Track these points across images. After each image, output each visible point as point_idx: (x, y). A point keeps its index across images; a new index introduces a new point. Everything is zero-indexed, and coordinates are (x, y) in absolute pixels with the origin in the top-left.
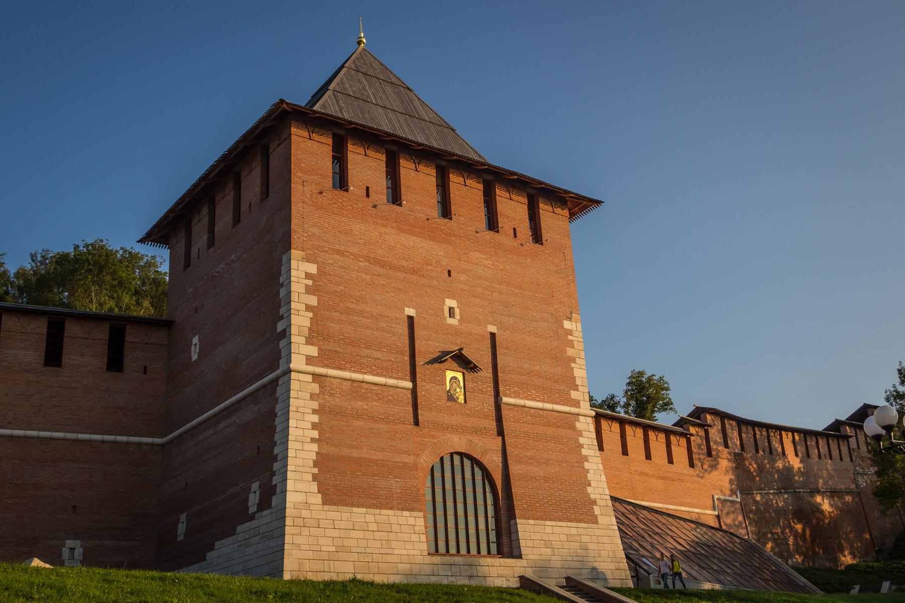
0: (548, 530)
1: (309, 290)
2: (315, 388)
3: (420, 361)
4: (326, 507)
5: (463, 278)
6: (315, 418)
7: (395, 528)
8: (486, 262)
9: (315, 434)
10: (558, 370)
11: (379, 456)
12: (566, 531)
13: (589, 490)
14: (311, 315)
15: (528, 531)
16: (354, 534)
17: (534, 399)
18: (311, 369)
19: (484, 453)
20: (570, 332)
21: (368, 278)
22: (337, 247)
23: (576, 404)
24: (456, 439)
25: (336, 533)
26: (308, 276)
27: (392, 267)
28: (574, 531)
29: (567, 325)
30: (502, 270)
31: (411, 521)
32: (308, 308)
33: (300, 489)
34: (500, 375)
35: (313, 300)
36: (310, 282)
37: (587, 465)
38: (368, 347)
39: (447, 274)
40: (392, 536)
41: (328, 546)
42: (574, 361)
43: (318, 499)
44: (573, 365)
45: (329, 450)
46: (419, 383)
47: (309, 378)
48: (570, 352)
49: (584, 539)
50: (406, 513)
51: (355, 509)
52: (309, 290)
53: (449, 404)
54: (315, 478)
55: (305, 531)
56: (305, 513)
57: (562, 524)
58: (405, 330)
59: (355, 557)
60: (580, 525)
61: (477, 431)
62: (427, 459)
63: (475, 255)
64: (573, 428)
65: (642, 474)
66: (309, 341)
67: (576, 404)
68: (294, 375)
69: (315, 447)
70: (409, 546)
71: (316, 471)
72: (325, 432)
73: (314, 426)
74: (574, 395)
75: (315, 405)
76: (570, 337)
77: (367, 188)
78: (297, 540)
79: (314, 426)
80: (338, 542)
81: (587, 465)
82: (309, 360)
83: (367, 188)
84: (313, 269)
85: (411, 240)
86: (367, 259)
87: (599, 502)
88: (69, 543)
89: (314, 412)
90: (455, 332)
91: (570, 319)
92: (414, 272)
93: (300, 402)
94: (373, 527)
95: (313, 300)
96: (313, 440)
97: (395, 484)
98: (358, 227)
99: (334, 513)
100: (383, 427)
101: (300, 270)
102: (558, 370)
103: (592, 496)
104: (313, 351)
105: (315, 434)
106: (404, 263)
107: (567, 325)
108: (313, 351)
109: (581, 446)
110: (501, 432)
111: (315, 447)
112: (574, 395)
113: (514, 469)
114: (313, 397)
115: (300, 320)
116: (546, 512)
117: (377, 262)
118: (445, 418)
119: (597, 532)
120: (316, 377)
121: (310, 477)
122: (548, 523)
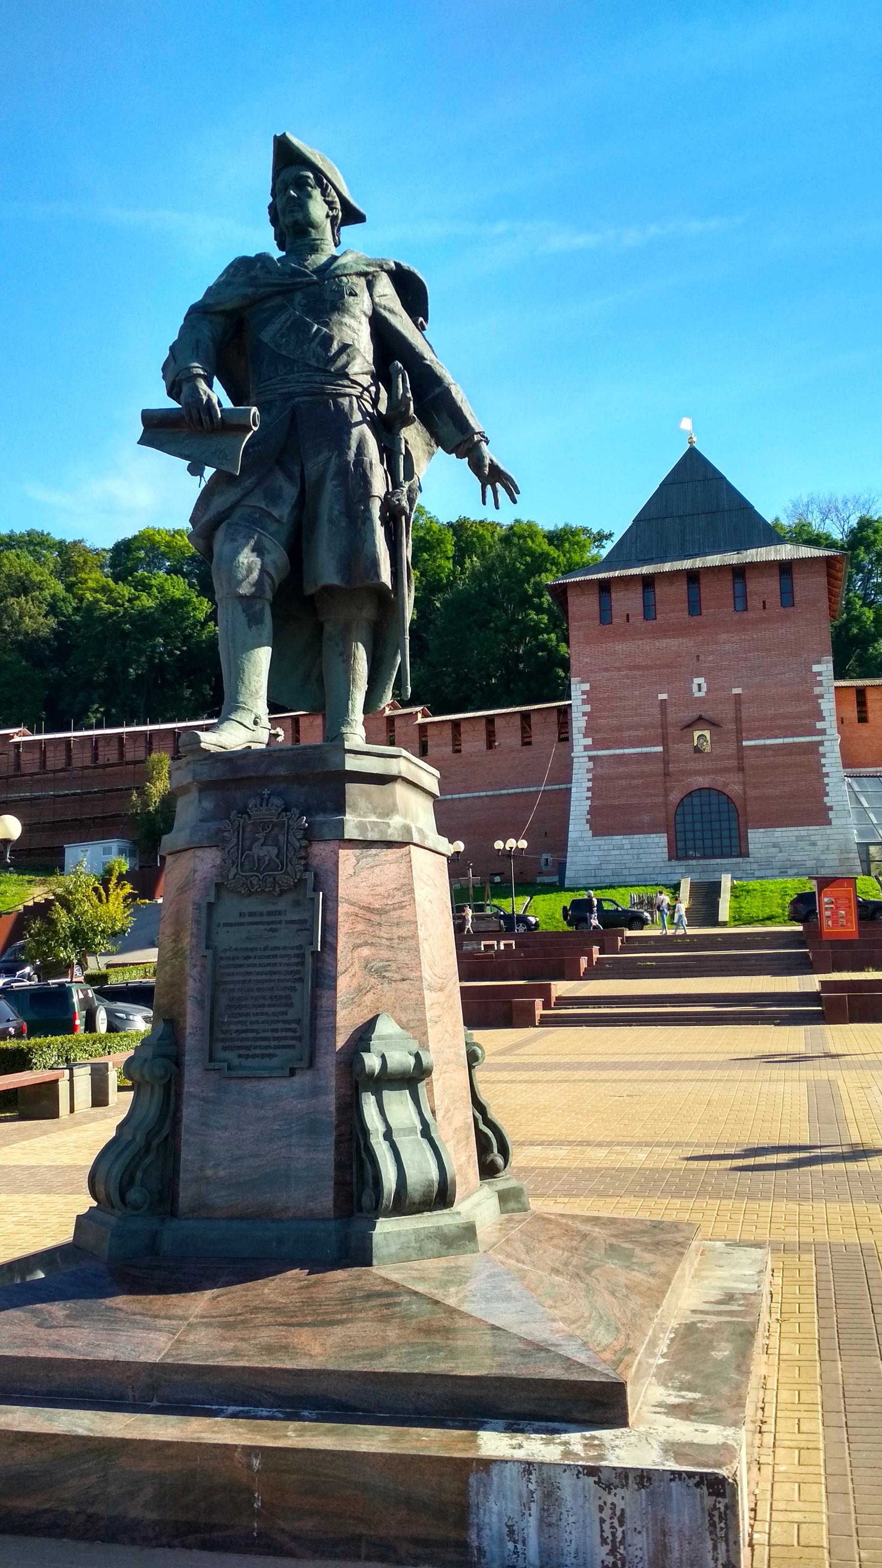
0: (777, 834)
1: (584, 702)
2: (591, 765)
3: (672, 730)
4: (595, 838)
6: (590, 784)
7: (644, 846)
8: (733, 639)
9: (590, 794)
10: (805, 708)
11: (635, 801)
12: (796, 833)
13: (826, 799)
14: (586, 718)
16: (613, 853)
17: (776, 737)
18: (586, 753)
19: (726, 785)
20: (820, 674)
22: (605, 666)
23: (823, 732)
24: (700, 779)
25: (601, 853)
26: (583, 693)
29: (816, 668)
30: (749, 641)
31: (657, 840)
32: (584, 714)
33: (578, 827)
34: (744, 725)
35: (587, 708)
36: (585, 697)
37: (826, 780)
38: (629, 728)
39: (695, 658)
40: (641, 851)
41: (594, 861)
42: (821, 696)
43: (590, 833)
44: (820, 701)
45: (597, 803)
46: (670, 745)
47: (587, 759)
48: (817, 690)
49: (813, 838)
50: (652, 835)
51: (615, 837)
52: (584, 702)
53: (697, 755)
54: (588, 821)
55: (580, 854)
56: (580, 843)
57: (792, 829)
59: (613, 866)
60: (810, 828)
62: (675, 797)
63: (724, 637)
64: (817, 752)
66: (585, 736)
68: (575, 760)
69: (589, 802)
70: (653, 856)
71: (589, 817)
73: (589, 789)
74: (819, 725)
75: (590, 776)
76: (819, 678)
77: (628, 615)
78: (574, 859)
79: (589, 789)
80: (603, 858)
81: (826, 780)
82: (586, 748)
83: (628, 615)
84: (586, 687)
85: (664, 643)
87: (834, 808)
89: (589, 780)
91: (819, 662)
92: (667, 666)
93: (580, 776)
94: (628, 846)
95: (587, 708)
96: (587, 798)
98: (620, 647)
99: (601, 841)
100: (635, 782)
101: (578, 689)
103: (828, 804)
104: (589, 741)
105: (590, 794)
106: (658, 662)
107: (816, 668)
108: (589, 741)
109: (824, 765)
111: (589, 802)
112: (819, 725)
113: (751, 793)
114: (588, 771)
115: (578, 722)
116: (774, 819)
118: (693, 766)
119: (829, 832)
120: (591, 758)
121: (585, 821)
122: (777, 829)
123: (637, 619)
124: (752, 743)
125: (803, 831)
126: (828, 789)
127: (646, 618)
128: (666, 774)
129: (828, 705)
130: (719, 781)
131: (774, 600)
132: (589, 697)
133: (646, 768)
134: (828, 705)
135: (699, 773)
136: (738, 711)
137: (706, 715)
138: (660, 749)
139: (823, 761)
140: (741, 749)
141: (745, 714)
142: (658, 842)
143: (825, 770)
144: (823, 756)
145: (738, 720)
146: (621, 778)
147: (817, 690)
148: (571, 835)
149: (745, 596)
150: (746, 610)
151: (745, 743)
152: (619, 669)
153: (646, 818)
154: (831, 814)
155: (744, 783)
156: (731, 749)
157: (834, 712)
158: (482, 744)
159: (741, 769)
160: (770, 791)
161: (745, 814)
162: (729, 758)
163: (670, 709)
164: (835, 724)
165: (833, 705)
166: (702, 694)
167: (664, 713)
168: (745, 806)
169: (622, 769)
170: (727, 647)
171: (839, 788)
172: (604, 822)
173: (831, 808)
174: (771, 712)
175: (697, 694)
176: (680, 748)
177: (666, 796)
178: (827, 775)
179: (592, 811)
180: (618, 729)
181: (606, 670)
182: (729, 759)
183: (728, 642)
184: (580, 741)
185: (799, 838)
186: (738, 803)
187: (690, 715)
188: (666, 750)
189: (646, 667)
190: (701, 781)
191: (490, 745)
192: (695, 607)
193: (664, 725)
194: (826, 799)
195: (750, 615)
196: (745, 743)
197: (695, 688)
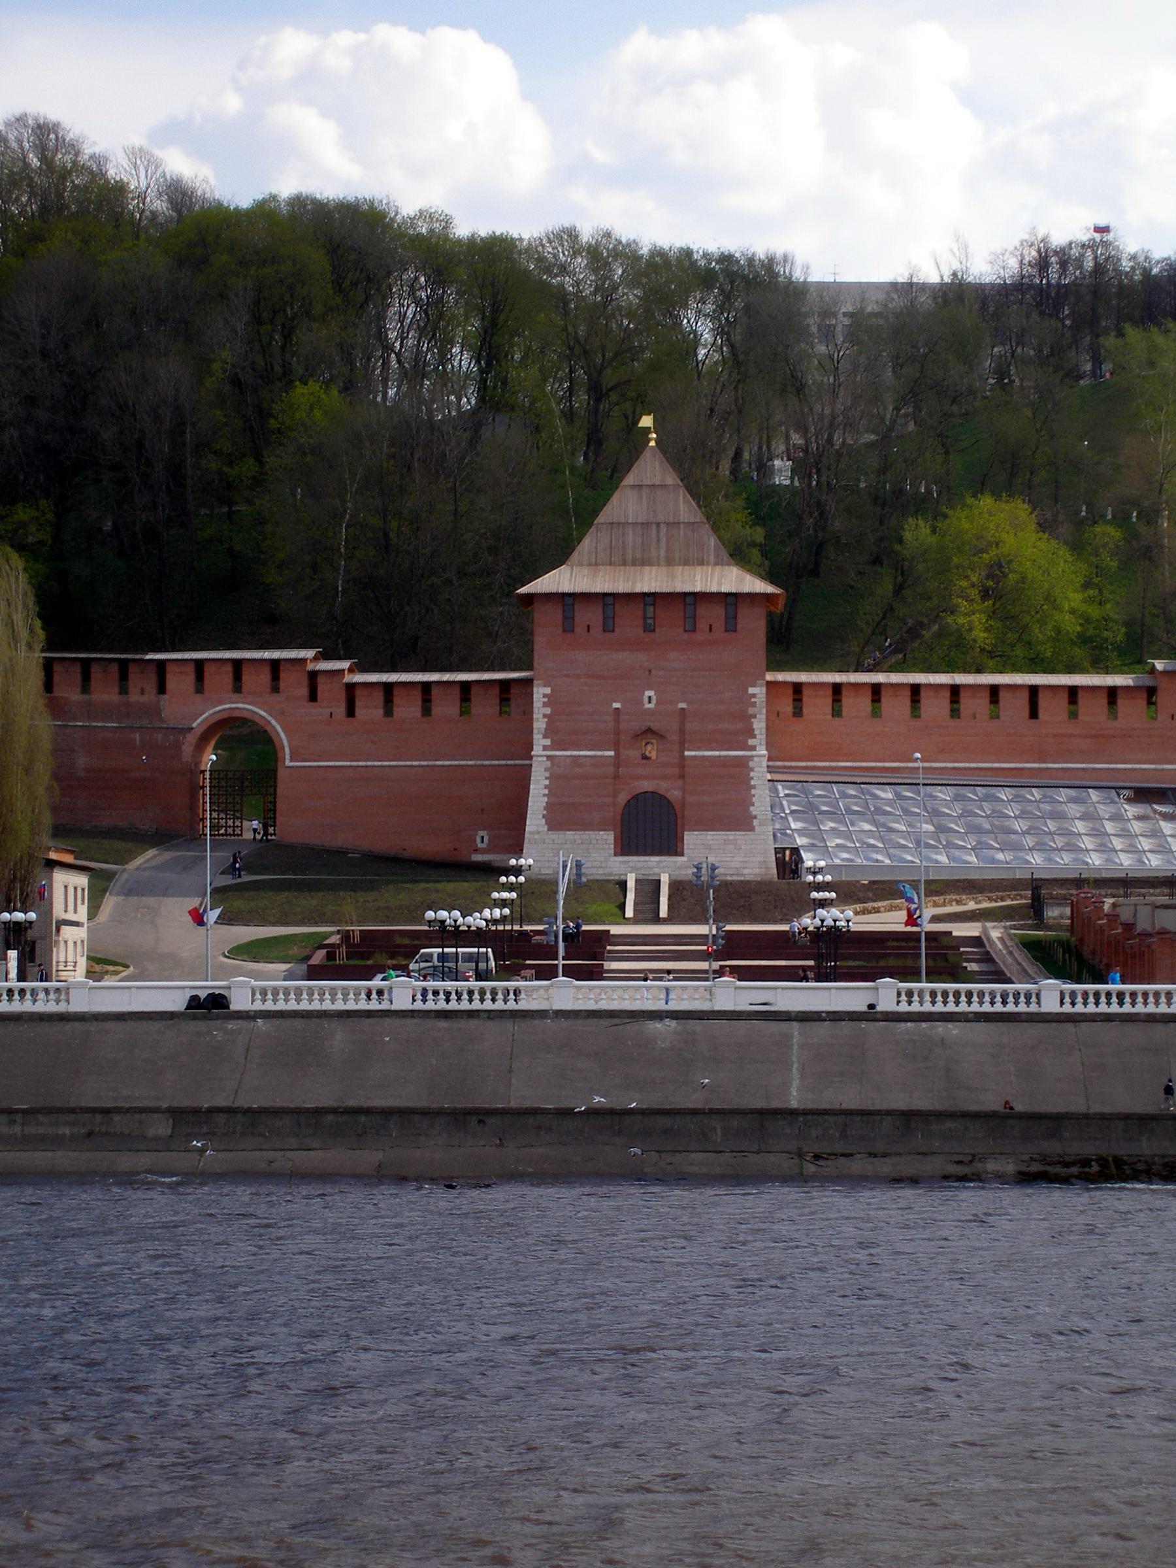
1: (545, 705)
3: (623, 737)
5: (661, 673)
6: (547, 782)
7: (594, 842)
10: (740, 725)
13: (752, 808)
15: (691, 839)
18: (545, 753)
20: (754, 696)
21: (585, 688)
26: (545, 696)
28: (731, 837)
29: (751, 690)
31: (605, 837)
32: (545, 716)
33: (535, 821)
35: (548, 711)
37: (753, 792)
42: (755, 716)
43: (546, 828)
46: (622, 750)
48: (751, 711)
52: (545, 705)
54: (544, 816)
61: (664, 777)
62: (623, 798)
64: (747, 766)
65: (1055, 736)
66: (545, 737)
67: (753, 748)
69: (546, 799)
72: (552, 791)
73: (546, 787)
74: (751, 742)
75: (547, 774)
79: (546, 787)
82: (545, 748)
84: (548, 690)
85: (619, 656)
88: (481, 833)
91: (754, 686)
95: (548, 711)
99: (554, 835)
102: (740, 725)
104: (548, 742)
105: (546, 792)
107: (751, 690)
108: (548, 742)
110: (682, 776)
111: (546, 799)
112: (751, 742)
113: (689, 799)
114: (546, 770)
115: (539, 724)
118: (640, 771)
123: (597, 632)
124: (693, 753)
125: (731, 835)
126: (754, 799)
128: (616, 777)
129: (759, 725)
131: (719, 625)
132: (550, 701)
134: (759, 725)
135: (645, 777)
136: (682, 723)
137: (655, 726)
138: (612, 753)
139: (752, 774)
140: (683, 758)
141: (688, 726)
143: (753, 783)
144: (752, 770)
145: (682, 731)
147: (751, 711)
148: (527, 829)
149: (694, 617)
150: (694, 631)
151: (686, 753)
152: (578, 677)
154: (755, 822)
155: (684, 790)
157: (764, 731)
158: (416, 710)
159: (682, 776)
161: (683, 818)
164: (764, 742)
165: (763, 725)
166: (651, 706)
168: (683, 811)
169: (577, 770)
171: (760, 803)
172: (558, 819)
173: (755, 817)
175: (648, 706)
176: (633, 754)
177: (615, 796)
178: (754, 787)
179: (549, 807)
181: (567, 676)
184: (540, 743)
188: (617, 755)
190: (647, 786)
191: (426, 711)
193: (617, 732)
194: (752, 808)
195: (700, 636)
196: (686, 753)
197: (646, 700)
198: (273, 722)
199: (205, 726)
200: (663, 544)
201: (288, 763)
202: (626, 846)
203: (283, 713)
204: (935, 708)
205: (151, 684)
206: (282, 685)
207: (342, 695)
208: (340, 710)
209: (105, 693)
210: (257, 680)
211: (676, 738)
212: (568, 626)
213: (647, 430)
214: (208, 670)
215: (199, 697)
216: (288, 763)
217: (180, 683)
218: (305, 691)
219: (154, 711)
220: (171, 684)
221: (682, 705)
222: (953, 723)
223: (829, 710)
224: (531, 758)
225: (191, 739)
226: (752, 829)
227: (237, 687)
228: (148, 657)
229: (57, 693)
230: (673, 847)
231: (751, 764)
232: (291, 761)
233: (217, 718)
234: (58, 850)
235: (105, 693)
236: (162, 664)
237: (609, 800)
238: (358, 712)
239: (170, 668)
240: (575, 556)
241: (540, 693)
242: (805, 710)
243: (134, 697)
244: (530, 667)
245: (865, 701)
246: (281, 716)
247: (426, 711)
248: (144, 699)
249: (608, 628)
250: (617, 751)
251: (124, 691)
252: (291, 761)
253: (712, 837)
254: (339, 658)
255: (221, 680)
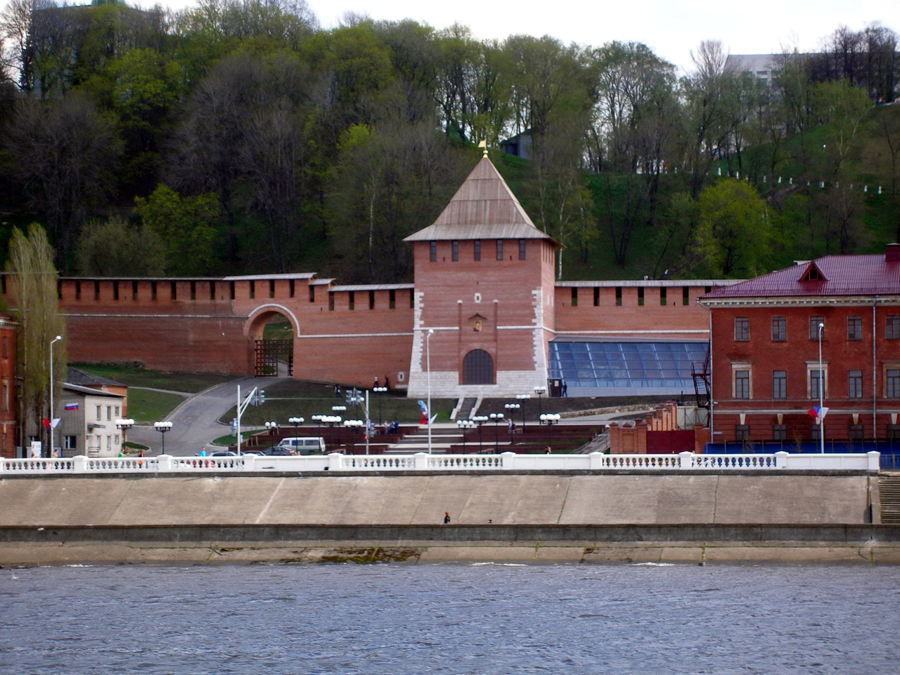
1: (421, 302)
3: (463, 319)
10: (527, 312)
11: (443, 354)
15: (501, 375)
23: (535, 324)
27: (453, 286)
35: (422, 305)
43: (421, 370)
48: (533, 303)
52: (421, 302)
58: (456, 309)
62: (463, 353)
63: (490, 273)
64: (531, 334)
66: (421, 319)
67: (535, 324)
74: (534, 321)
82: (421, 326)
84: (422, 294)
86: (444, 286)
88: (401, 373)
90: (478, 305)
91: (535, 289)
92: (462, 286)
95: (422, 305)
97: (449, 363)
98: (440, 275)
100: (446, 344)
102: (527, 312)
104: (422, 322)
107: (534, 292)
110: (496, 340)
112: (534, 321)
113: (500, 353)
115: (418, 312)
117: (448, 286)
123: (449, 261)
125: (522, 373)
127: (453, 260)
128: (460, 341)
130: (485, 346)
131: (516, 256)
132: (424, 300)
133: (451, 338)
135: (475, 341)
137: (480, 313)
138: (457, 328)
140: (496, 330)
141: (499, 313)
142: (455, 375)
145: (496, 315)
146: (438, 342)
153: (449, 363)
154: (536, 365)
156: (491, 331)
159: (496, 340)
160: (508, 352)
162: (491, 334)
163: (463, 308)
167: (460, 310)
170: (492, 279)
174: (511, 313)
175: (477, 302)
176: (469, 328)
177: (459, 352)
180: (437, 317)
182: (491, 334)
183: (493, 276)
184: (418, 324)
185: (520, 376)
186: (493, 358)
187: (472, 312)
188: (460, 329)
189: (453, 286)
190: (476, 346)
191: (372, 305)
192: (477, 257)
193: (460, 316)
195: (503, 263)
198: (291, 313)
199: (255, 316)
200: (488, 212)
201: (299, 336)
202: (467, 378)
203: (296, 309)
204: (652, 299)
205: (227, 293)
206: (296, 293)
207: (327, 298)
208: (326, 306)
209: (203, 299)
210: (282, 291)
211: (492, 319)
212: (433, 258)
213: (483, 149)
214: (257, 285)
215: (252, 301)
216: (299, 336)
217: (242, 292)
218: (307, 296)
219: (229, 308)
220: (237, 293)
221: (496, 301)
222: (663, 308)
223: (592, 302)
224: (413, 331)
225: (247, 325)
226: (534, 369)
227: (272, 295)
228: (226, 279)
229: (178, 299)
230: (490, 379)
231: (534, 333)
232: (301, 334)
233: (261, 312)
234: (108, 386)
235: (203, 299)
236: (232, 283)
237: (455, 354)
238: (337, 307)
239: (236, 285)
240: (439, 220)
241: (418, 295)
242: (579, 303)
243: (218, 301)
244: (412, 282)
245: (612, 297)
246: (295, 310)
247: (372, 305)
248: (224, 302)
249: (454, 259)
250: (460, 327)
251: (213, 297)
252: (301, 334)
253: (513, 374)
254: (326, 278)
255: (262, 291)
